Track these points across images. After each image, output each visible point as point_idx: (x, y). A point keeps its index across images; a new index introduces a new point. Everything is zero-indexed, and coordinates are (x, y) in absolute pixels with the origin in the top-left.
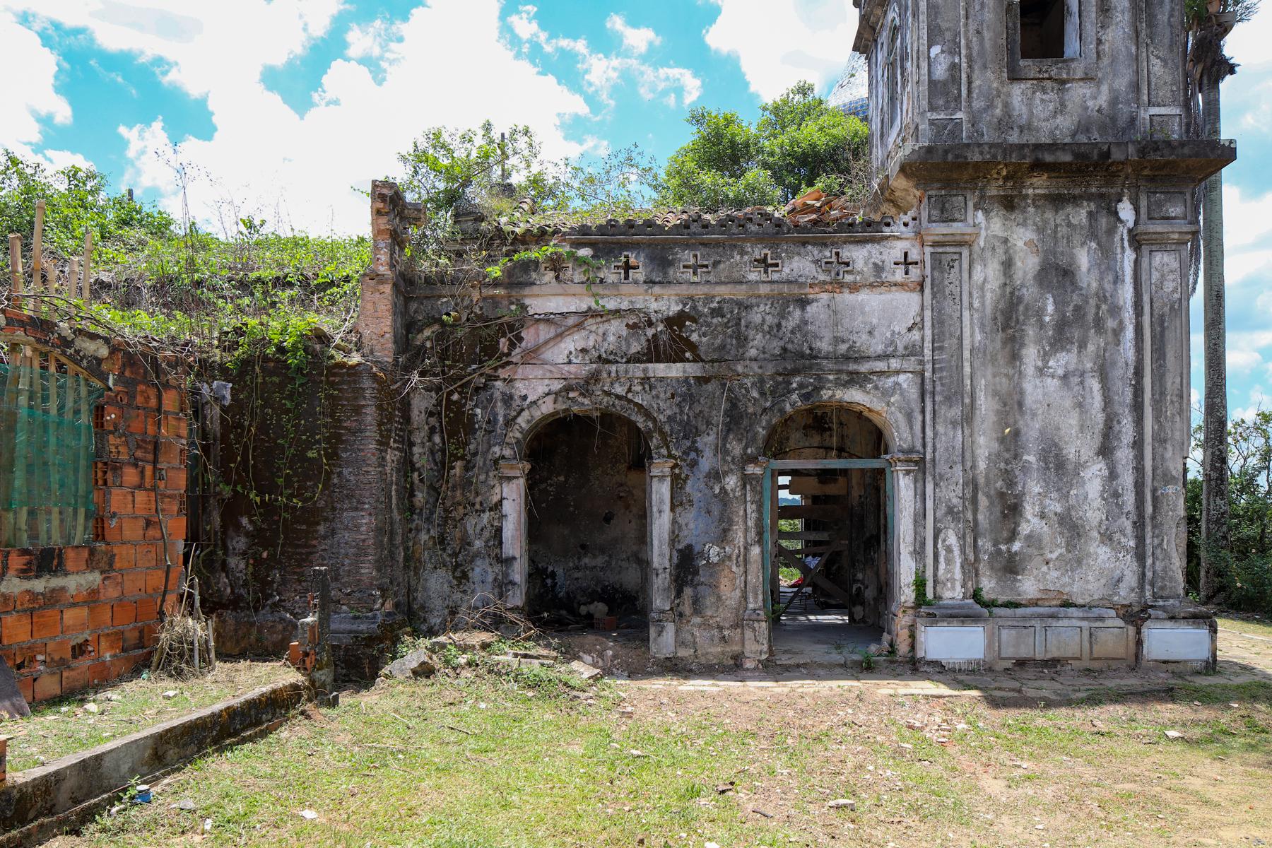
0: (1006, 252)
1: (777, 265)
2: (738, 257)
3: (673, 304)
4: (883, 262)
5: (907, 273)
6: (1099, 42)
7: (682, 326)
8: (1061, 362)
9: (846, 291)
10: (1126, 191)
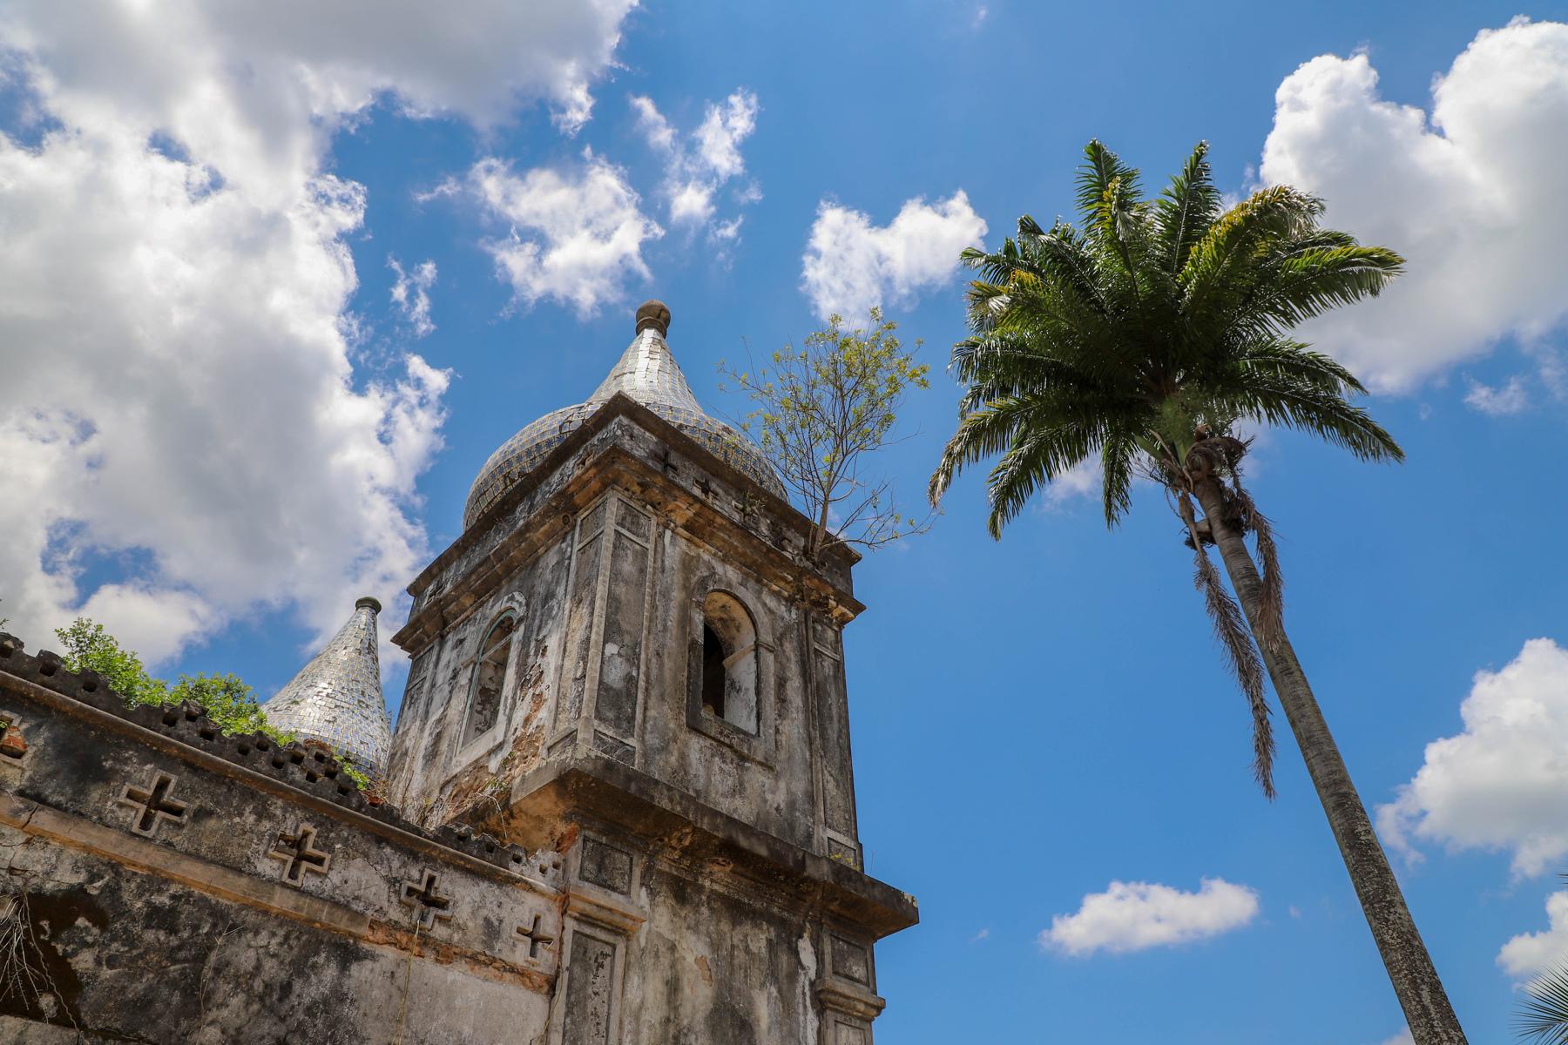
0: (673, 966)
1: (319, 861)
2: (251, 819)
3: (67, 864)
4: (501, 921)
5: (533, 954)
6: (777, 731)
7: (63, 922)
9: (430, 955)
10: (808, 925)
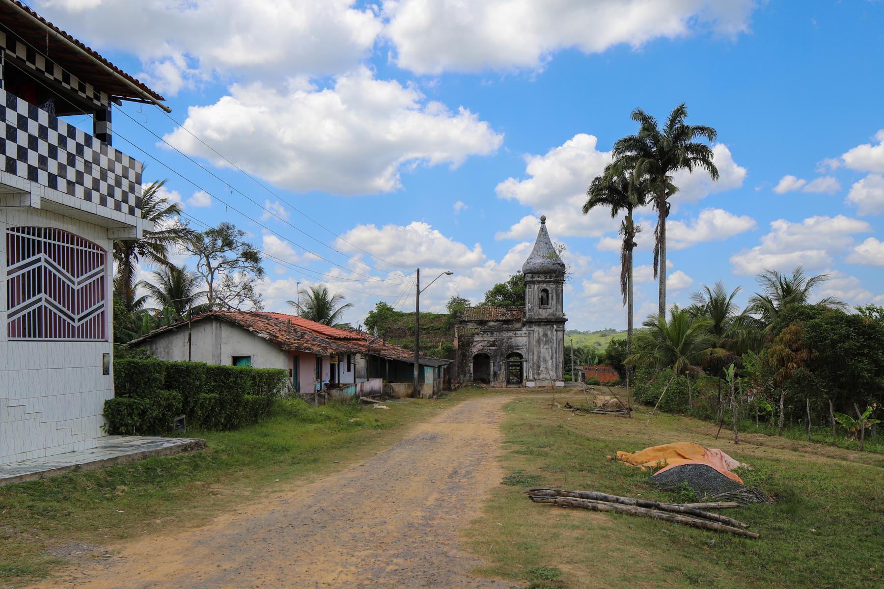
8: (546, 347)
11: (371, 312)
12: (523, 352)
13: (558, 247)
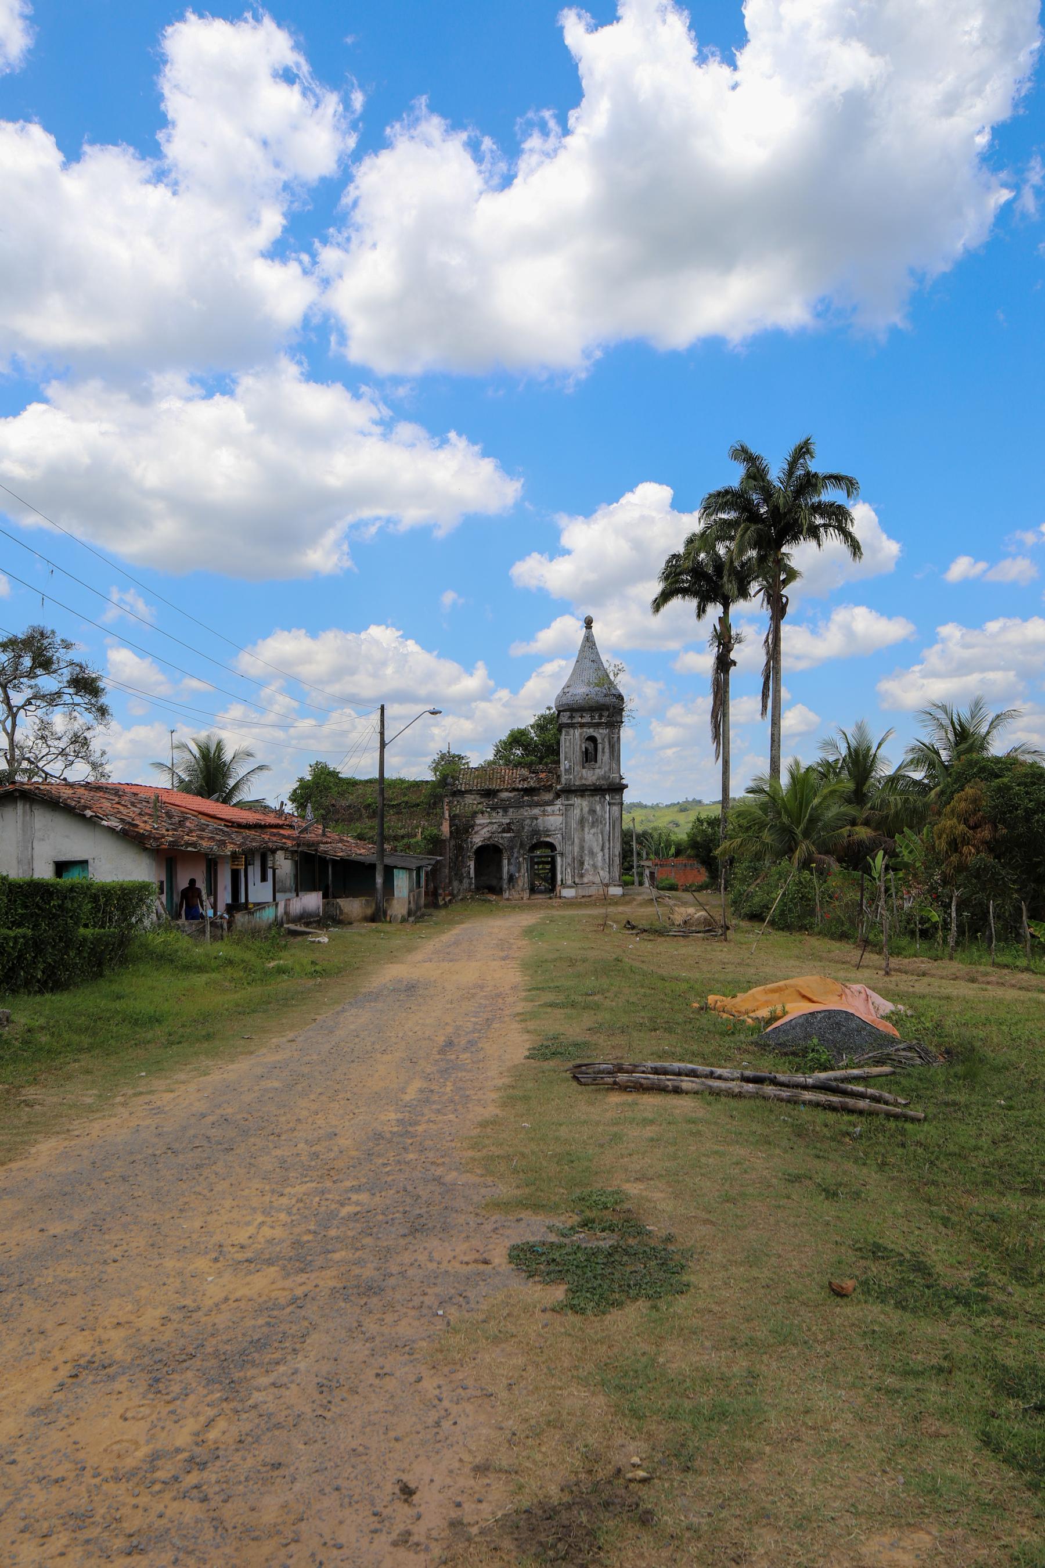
8: (593, 831)
11: (301, 780)
12: (556, 840)
13: (612, 668)
